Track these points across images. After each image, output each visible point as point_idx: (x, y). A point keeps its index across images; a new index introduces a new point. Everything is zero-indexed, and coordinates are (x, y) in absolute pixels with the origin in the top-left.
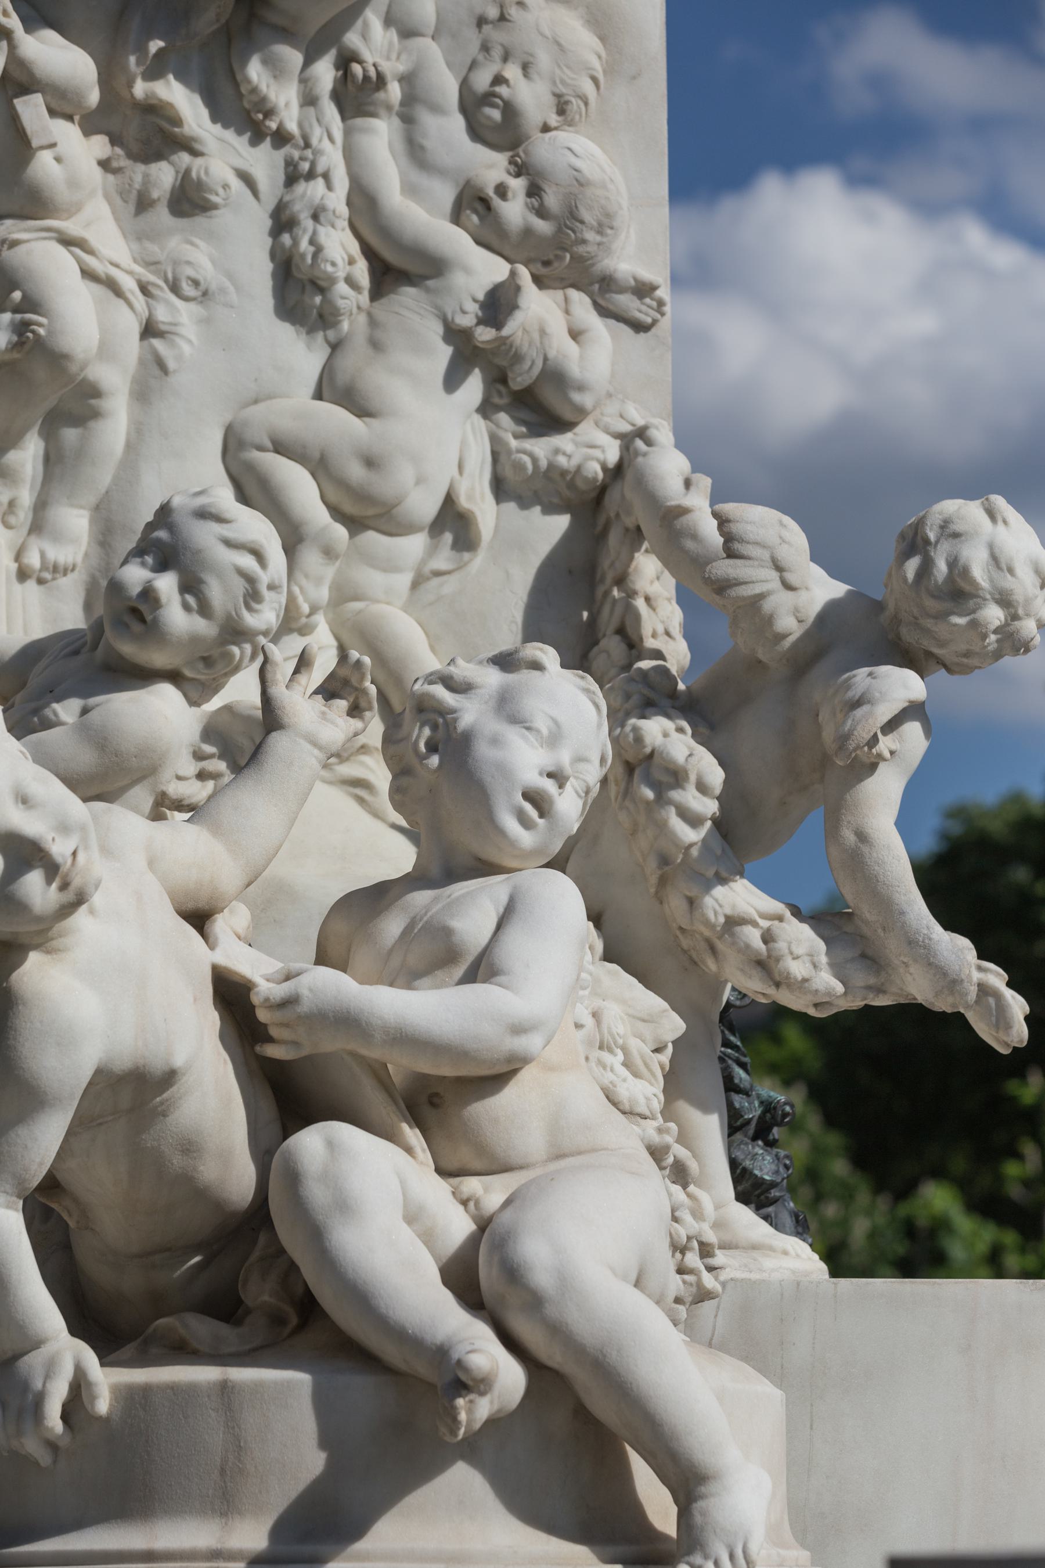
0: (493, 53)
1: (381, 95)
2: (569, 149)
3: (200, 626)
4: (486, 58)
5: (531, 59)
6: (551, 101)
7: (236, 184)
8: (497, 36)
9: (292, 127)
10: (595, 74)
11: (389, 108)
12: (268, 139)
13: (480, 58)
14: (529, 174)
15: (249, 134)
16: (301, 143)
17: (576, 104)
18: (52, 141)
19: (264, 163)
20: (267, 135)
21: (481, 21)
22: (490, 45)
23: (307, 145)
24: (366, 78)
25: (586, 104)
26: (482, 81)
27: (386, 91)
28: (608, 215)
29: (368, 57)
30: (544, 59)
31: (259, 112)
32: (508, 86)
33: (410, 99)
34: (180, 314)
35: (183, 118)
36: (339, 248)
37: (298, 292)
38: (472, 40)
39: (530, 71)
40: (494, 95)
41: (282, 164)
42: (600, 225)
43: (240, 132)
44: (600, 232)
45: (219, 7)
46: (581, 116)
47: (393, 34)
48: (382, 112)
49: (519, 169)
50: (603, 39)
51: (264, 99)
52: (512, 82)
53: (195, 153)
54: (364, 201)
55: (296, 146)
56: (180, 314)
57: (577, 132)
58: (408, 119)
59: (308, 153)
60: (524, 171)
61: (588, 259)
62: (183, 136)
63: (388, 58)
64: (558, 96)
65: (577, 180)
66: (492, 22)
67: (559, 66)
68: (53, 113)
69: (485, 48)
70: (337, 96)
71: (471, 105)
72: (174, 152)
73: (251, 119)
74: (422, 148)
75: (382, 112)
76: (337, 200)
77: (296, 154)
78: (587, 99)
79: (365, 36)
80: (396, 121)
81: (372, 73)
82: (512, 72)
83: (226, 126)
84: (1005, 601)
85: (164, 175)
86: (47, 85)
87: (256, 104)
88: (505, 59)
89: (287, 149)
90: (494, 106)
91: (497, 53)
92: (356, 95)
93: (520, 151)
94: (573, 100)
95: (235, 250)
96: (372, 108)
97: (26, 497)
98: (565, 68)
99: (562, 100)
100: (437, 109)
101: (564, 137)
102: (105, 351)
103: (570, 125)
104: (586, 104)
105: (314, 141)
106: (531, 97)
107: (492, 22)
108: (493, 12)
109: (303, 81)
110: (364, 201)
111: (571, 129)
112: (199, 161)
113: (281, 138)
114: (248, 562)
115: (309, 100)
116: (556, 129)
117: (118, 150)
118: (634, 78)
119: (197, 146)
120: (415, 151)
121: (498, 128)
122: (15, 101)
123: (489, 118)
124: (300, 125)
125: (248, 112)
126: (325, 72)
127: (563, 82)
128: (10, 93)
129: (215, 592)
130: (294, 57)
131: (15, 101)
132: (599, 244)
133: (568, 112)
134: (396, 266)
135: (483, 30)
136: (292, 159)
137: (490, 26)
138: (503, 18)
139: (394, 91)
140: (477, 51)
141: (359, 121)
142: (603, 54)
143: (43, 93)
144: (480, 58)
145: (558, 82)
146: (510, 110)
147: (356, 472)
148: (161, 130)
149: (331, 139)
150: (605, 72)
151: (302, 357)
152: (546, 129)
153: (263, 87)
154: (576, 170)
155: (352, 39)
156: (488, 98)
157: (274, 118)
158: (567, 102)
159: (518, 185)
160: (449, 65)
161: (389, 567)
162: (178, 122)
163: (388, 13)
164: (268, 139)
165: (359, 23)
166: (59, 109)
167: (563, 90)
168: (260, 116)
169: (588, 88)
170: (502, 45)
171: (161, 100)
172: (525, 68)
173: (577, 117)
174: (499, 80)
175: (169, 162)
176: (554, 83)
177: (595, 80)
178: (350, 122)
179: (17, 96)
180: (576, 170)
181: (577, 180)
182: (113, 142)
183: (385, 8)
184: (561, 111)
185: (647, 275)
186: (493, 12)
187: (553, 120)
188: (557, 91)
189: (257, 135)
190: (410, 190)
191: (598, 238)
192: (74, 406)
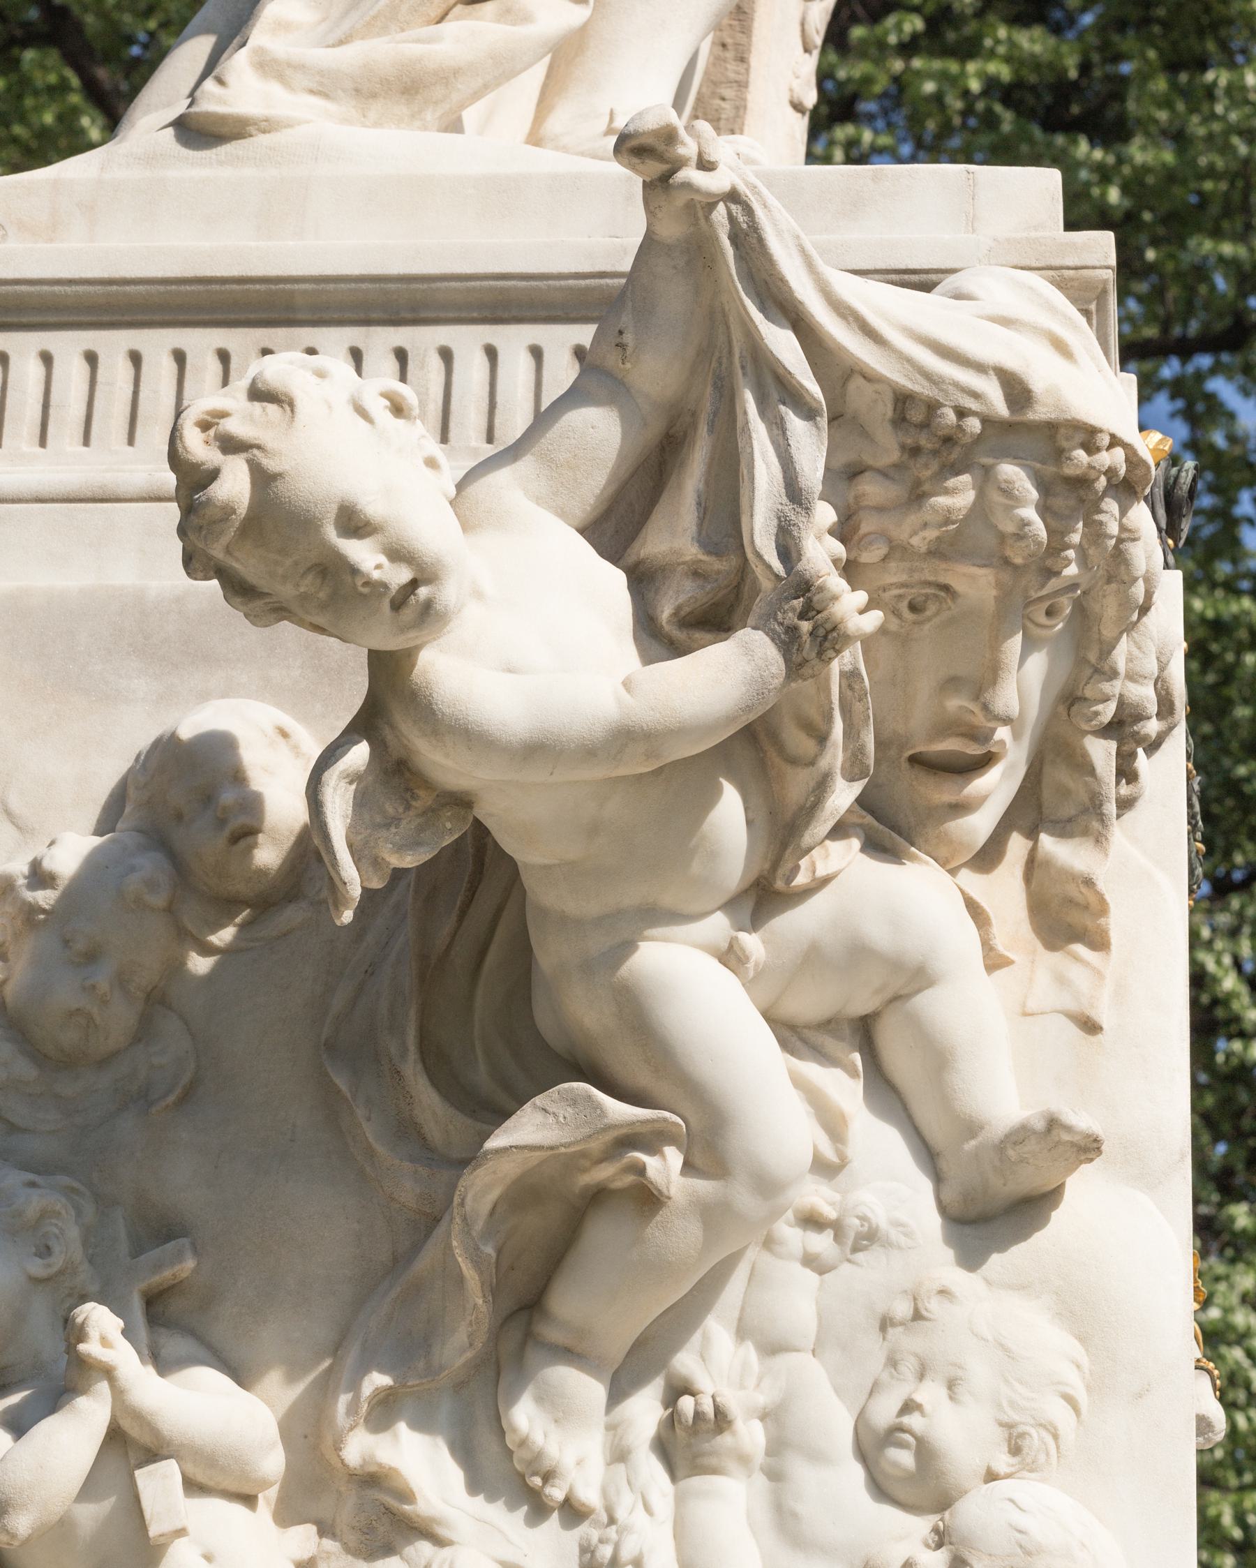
0: (902, 1368)
1: (725, 1440)
2: (1011, 1501)
4: (892, 1377)
5: (960, 1373)
6: (1000, 1434)
8: (909, 1342)
9: (589, 1495)
11: (744, 1459)
12: (555, 1515)
13: (885, 1377)
14: (951, 1543)
15: (526, 1508)
16: (605, 1519)
17: (1036, 1439)
18: (180, 1527)
20: (553, 1510)
21: (885, 1324)
22: (898, 1357)
23: (612, 1521)
24: (698, 1415)
25: (1056, 1437)
26: (884, 1412)
27: (734, 1434)
29: (704, 1383)
31: (535, 1474)
32: (923, 1414)
33: (777, 1447)
35: (415, 1490)
38: (874, 1349)
39: (959, 1390)
40: (901, 1429)
41: (577, 1550)
43: (512, 1506)
45: (471, 1324)
46: (1048, 1454)
47: (750, 1351)
48: (731, 1465)
50: (1083, 1339)
51: (539, 1456)
52: (927, 1407)
53: (439, 1542)
55: (596, 1524)
58: (775, 1475)
59: (612, 1532)
60: (946, 1539)
62: (418, 1516)
63: (742, 1387)
64: (1009, 1426)
65: (1021, 1546)
66: (902, 1324)
67: (1006, 1381)
68: (193, 1487)
69: (892, 1362)
70: (664, 1448)
71: (870, 1447)
72: (410, 1543)
73: (522, 1485)
74: (795, 1515)
75: (731, 1465)
77: (595, 1535)
78: (1055, 1429)
79: (703, 1357)
80: (760, 1481)
81: (709, 1409)
82: (930, 1394)
83: (492, 1498)
86: (182, 1445)
87: (530, 1463)
88: (921, 1376)
89: (586, 1530)
90: (902, 1445)
91: (908, 1367)
92: (687, 1444)
93: (947, 1514)
94: (1033, 1431)
96: (713, 1461)
98: (1017, 1385)
99: (1015, 1432)
100: (817, 1456)
101: (1020, 1488)
103: (1031, 1471)
104: (1056, 1437)
105: (621, 1514)
106: (959, 1431)
107: (902, 1324)
108: (902, 1309)
109: (611, 1428)
111: (1033, 1475)
112: (446, 1552)
113: (573, 1512)
115: (619, 1455)
116: (1008, 1476)
117: (329, 1544)
119: (442, 1532)
121: (910, 1478)
122: (137, 1473)
123: (895, 1465)
124: (604, 1493)
125: (522, 1477)
126: (645, 1410)
127: (1012, 1404)
128: (132, 1462)
130: (586, 1388)
131: (137, 1473)
133: (1025, 1450)
135: (889, 1337)
136: (589, 1545)
137: (900, 1329)
138: (917, 1316)
139: (750, 1434)
140: (881, 1367)
141: (697, 1482)
142: (1085, 1361)
143: (179, 1459)
144: (885, 1377)
145: (1005, 1404)
146: (924, 1451)
148: (388, 1511)
149: (648, 1509)
150: (1089, 1389)
152: (991, 1476)
153: (538, 1439)
154: (1020, 1532)
155: (685, 1361)
156: (892, 1435)
157: (557, 1481)
158: (1022, 1435)
160: (837, 1390)
162: (407, 1496)
163: (740, 1319)
164: (555, 1515)
165: (696, 1338)
166: (211, 1484)
167: (1014, 1416)
168: (537, 1481)
170: (916, 1355)
171: (380, 1465)
172: (951, 1385)
173: (1042, 1458)
174: (909, 1407)
175: (402, 1558)
176: (999, 1406)
177: (1070, 1400)
178: (684, 1484)
179: (140, 1466)
180: (1020, 1532)
181: (1021, 1546)
182: (322, 1533)
183: (736, 1314)
184: (1015, 1450)
186: (902, 1309)
187: (1003, 1462)
188: (1006, 1419)
189: (538, 1509)
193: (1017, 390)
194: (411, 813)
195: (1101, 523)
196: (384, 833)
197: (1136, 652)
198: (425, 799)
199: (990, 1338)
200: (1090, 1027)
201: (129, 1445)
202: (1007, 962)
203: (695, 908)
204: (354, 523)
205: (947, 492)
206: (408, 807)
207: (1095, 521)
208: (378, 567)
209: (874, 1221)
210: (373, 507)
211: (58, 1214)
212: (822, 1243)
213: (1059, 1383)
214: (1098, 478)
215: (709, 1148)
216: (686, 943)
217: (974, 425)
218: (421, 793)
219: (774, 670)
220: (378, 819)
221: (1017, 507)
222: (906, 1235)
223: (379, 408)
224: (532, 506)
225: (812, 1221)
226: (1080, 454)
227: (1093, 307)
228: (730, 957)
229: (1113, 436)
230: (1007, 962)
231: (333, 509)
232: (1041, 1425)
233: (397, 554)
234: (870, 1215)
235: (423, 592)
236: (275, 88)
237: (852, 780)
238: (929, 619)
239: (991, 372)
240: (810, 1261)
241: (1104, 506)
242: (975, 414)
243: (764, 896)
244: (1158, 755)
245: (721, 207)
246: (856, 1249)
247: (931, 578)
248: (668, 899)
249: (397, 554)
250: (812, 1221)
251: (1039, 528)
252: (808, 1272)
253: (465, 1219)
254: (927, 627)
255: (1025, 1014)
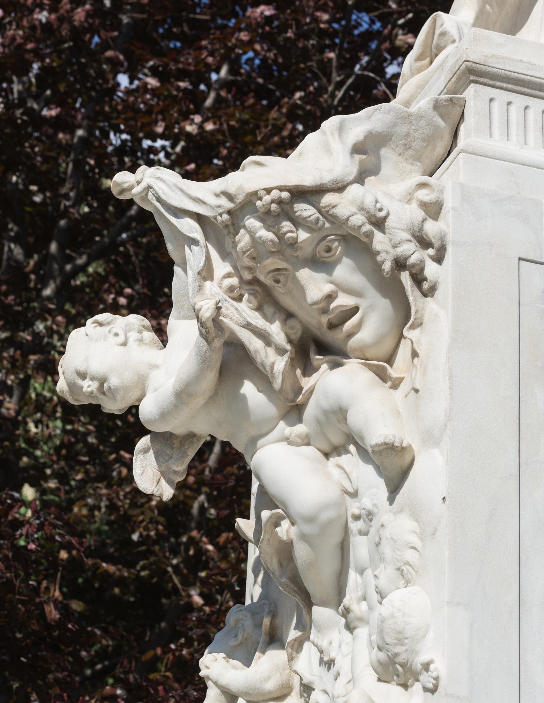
10: (413, 545)
27: (352, 611)
28: (400, 633)
42: (399, 640)
44: (402, 645)
48: (357, 623)
50: (417, 521)
57: (413, 585)
61: (407, 663)
118: (434, 534)
132: (406, 651)
173: (410, 576)
188: (397, 567)
191: (404, 648)
194: (175, 450)
195: (299, 216)
196: (170, 461)
197: (391, 237)
198: (176, 443)
199: (389, 537)
200: (417, 391)
202: (401, 379)
203: (264, 430)
204: (83, 376)
205: (238, 243)
206: (173, 448)
207: (297, 216)
208: (89, 386)
209: (366, 508)
211: (242, 619)
213: (408, 544)
214: (270, 207)
216: (269, 444)
217: (226, 217)
218: (175, 441)
219: (201, 345)
220: (167, 458)
221: (255, 234)
222: (377, 508)
224: (176, 321)
225: (357, 518)
226: (259, 203)
227: (472, 78)
229: (265, 189)
230: (401, 379)
231: (75, 374)
232: (405, 564)
234: (365, 507)
235: (105, 385)
237: (283, 355)
238: (287, 281)
239: (221, 195)
240: (361, 533)
241: (295, 209)
242: (223, 213)
243: (294, 411)
244: (445, 262)
245: (150, 193)
246: (371, 520)
247: (267, 271)
248: (253, 432)
249: (92, 379)
250: (357, 518)
251: (270, 236)
252: (362, 537)
253: (273, 574)
254: (289, 284)
255: (406, 396)
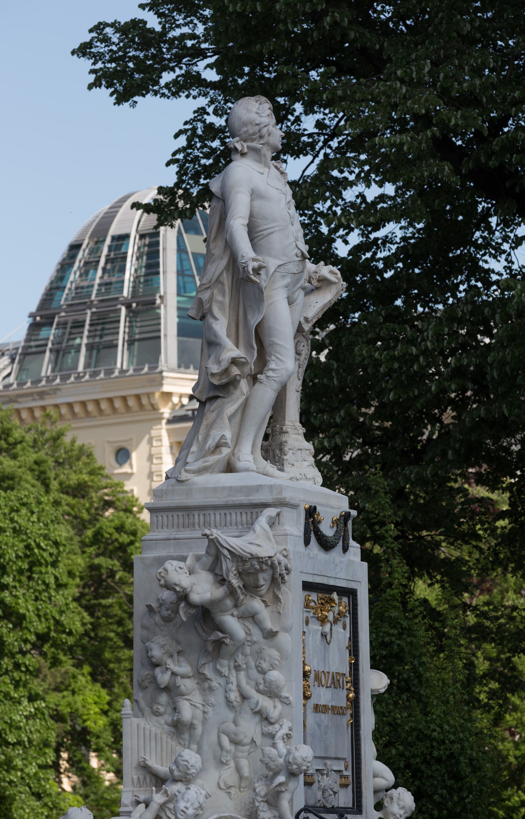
3: (180, 773)
7: (217, 685)
11: (243, 669)
19: (222, 681)
30: (267, 658)
34: (209, 709)
36: (234, 696)
37: (229, 703)
49: (264, 679)
54: (239, 686)
56: (209, 709)
71: (257, 667)
73: (219, 673)
76: (234, 687)
84: (296, 764)
85: (206, 685)
92: (237, 668)
95: (217, 698)
97: (187, 743)
102: (193, 717)
106: (265, 665)
110: (239, 686)
114: (186, 763)
120: (248, 677)
126: (232, 664)
129: (181, 768)
134: (244, 697)
146: (261, 668)
147: (233, 736)
151: (231, 715)
159: (262, 682)
161: (242, 752)
169: (277, 662)
184: (272, 666)
185: (287, 695)
190: (248, 683)
192: (192, 727)
193: (251, 554)
201: (174, 674)
210: (178, 583)
212: (249, 643)
215: (232, 637)
223: (178, 569)
228: (232, 615)
233: (181, 588)
236: (188, 474)
